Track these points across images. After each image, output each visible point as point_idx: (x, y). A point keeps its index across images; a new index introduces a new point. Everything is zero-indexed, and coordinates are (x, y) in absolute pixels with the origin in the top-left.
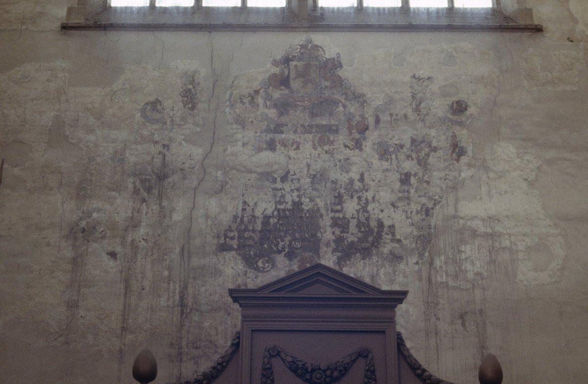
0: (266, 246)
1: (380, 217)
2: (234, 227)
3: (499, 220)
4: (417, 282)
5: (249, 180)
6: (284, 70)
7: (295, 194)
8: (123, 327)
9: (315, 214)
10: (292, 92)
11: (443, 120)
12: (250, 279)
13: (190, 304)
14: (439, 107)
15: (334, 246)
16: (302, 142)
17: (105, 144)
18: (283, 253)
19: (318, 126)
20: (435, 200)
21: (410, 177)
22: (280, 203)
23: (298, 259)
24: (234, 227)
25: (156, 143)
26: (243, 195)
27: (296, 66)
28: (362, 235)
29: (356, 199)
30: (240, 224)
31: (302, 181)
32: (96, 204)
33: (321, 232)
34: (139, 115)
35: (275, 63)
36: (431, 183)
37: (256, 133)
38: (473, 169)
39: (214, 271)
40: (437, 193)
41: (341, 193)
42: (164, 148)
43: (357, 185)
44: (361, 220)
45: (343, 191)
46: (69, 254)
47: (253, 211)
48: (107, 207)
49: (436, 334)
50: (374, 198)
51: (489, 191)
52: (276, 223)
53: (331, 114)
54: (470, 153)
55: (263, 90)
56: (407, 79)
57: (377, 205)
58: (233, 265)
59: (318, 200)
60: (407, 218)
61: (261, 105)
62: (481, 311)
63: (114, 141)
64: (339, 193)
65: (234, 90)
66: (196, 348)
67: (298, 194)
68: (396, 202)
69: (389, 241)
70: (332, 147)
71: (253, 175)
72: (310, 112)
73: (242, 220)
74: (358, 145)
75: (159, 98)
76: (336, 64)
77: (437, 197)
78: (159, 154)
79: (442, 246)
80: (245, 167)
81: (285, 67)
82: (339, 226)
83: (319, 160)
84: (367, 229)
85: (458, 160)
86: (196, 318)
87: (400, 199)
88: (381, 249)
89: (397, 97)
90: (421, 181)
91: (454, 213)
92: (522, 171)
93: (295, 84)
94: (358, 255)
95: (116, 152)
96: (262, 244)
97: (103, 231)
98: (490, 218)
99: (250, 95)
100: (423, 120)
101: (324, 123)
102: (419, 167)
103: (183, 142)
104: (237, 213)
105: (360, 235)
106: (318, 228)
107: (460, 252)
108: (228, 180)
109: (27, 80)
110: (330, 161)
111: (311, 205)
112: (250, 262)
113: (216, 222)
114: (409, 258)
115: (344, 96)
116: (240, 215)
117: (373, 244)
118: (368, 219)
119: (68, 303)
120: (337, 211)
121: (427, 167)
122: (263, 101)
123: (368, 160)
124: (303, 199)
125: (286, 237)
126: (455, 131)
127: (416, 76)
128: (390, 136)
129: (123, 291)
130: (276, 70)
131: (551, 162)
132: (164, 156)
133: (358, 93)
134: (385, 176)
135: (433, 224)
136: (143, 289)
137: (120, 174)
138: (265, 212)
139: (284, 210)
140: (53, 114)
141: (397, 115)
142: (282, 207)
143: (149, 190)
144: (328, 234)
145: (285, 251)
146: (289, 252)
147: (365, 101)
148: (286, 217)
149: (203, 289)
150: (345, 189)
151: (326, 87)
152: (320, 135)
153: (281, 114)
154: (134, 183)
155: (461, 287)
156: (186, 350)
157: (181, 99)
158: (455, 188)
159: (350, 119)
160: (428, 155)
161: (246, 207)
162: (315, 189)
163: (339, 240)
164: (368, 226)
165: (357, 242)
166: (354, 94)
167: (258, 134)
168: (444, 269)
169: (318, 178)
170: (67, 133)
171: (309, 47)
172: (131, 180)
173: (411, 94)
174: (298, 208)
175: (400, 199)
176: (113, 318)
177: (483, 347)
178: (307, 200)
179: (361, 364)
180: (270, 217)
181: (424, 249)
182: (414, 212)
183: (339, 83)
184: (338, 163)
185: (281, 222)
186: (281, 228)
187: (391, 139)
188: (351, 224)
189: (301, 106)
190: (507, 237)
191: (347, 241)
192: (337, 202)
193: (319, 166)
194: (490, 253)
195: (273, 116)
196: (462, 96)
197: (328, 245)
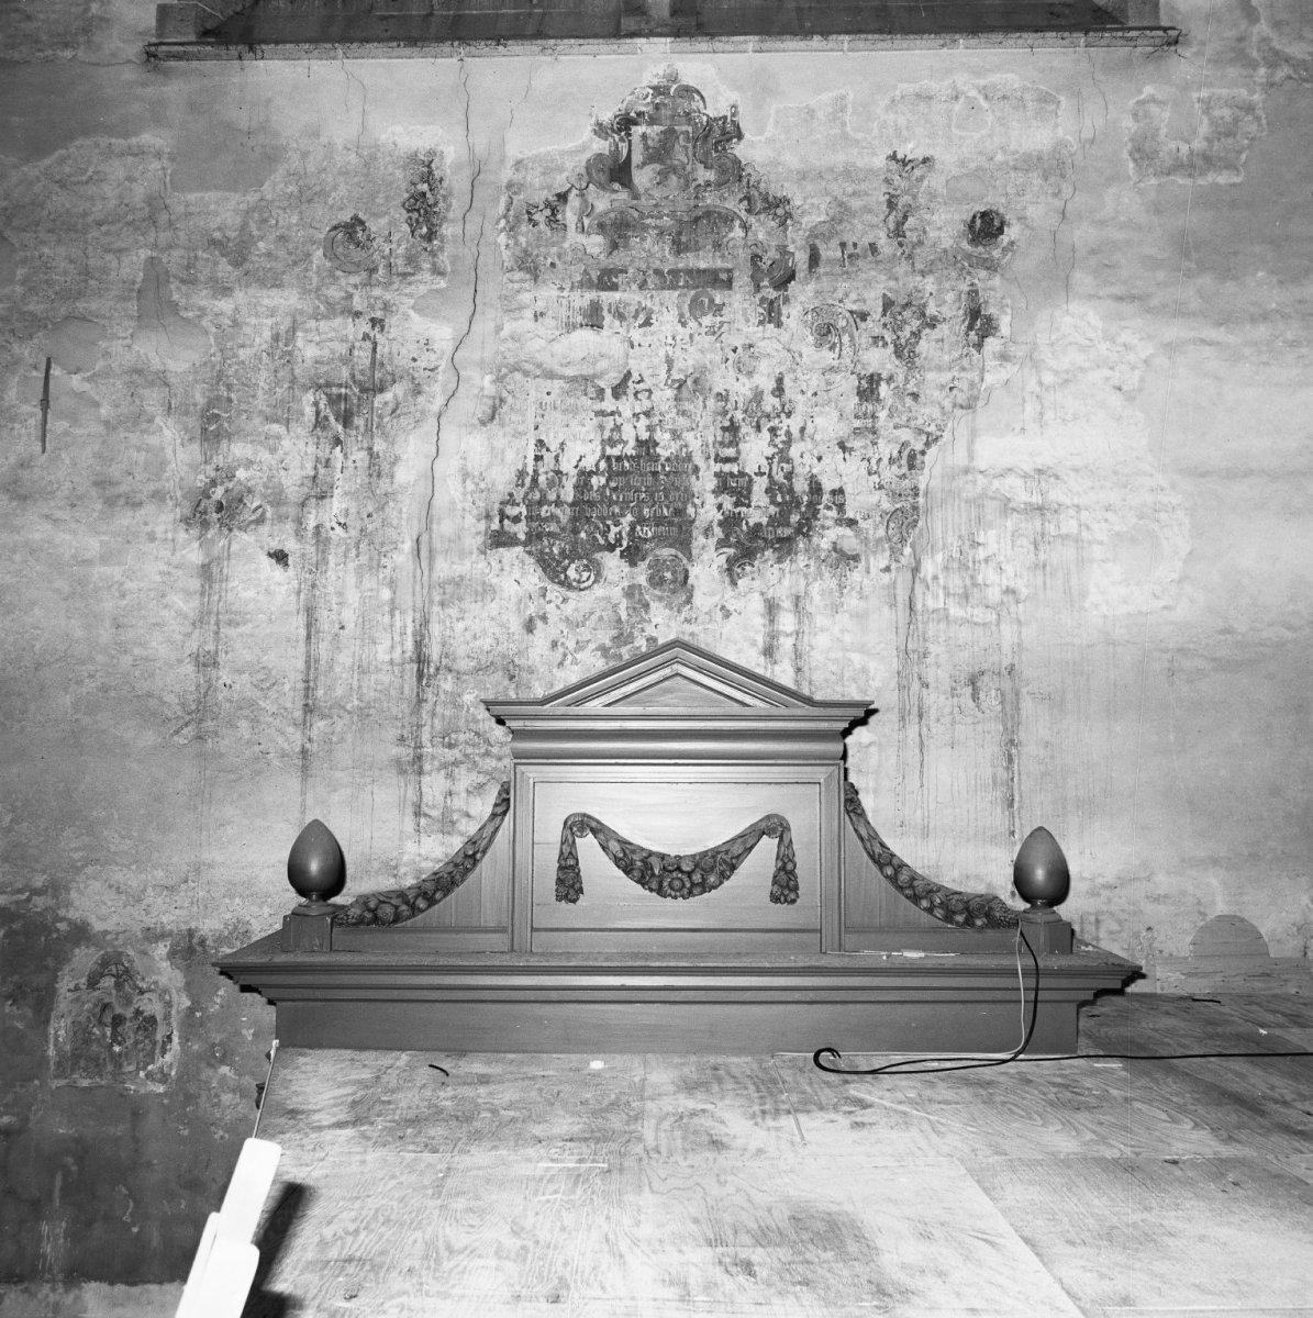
0: (583, 535)
1: (815, 471)
2: (519, 494)
3: (1057, 478)
4: (886, 609)
5: (548, 394)
6: (620, 145)
7: (644, 422)
8: (306, 705)
9: (683, 464)
10: (636, 197)
11: (950, 259)
12: (552, 605)
13: (435, 657)
14: (944, 226)
15: (722, 536)
16: (656, 308)
17: (253, 321)
18: (618, 550)
19: (689, 272)
20: (928, 434)
21: (878, 385)
22: (612, 442)
23: (647, 562)
24: (519, 496)
25: (358, 314)
26: (536, 428)
27: (644, 137)
28: (777, 510)
29: (766, 435)
30: (531, 489)
31: (656, 395)
32: (239, 450)
33: (695, 506)
34: (320, 252)
35: (601, 130)
36: (922, 399)
37: (562, 289)
38: (1009, 365)
39: (480, 589)
40: (933, 420)
41: (735, 420)
42: (373, 327)
43: (770, 403)
44: (776, 478)
45: (739, 416)
46: (195, 556)
47: (557, 461)
48: (264, 455)
49: (921, 716)
50: (803, 430)
51: (1041, 414)
52: (604, 487)
53: (717, 246)
54: (1005, 329)
55: (574, 192)
56: (880, 161)
57: (809, 445)
58: (517, 575)
59: (689, 437)
60: (870, 474)
61: (572, 227)
62: (1011, 670)
63: (272, 312)
64: (731, 420)
65: (515, 193)
66: (450, 746)
67: (648, 423)
68: (848, 440)
69: (829, 523)
70: (719, 319)
71: (557, 384)
72: (674, 242)
73: (535, 481)
74: (772, 314)
75: (361, 215)
76: (724, 133)
77: (932, 429)
78: (364, 339)
79: (939, 533)
80: (539, 366)
81: (622, 140)
82: (732, 492)
83: (691, 349)
84: (788, 497)
85: (979, 346)
86: (447, 684)
87: (857, 432)
88: (815, 540)
89: (856, 204)
90: (899, 393)
91: (966, 462)
92: (1112, 368)
93: (643, 177)
94: (768, 553)
95: (276, 338)
96: (576, 532)
97: (260, 507)
98: (1040, 471)
99: (548, 204)
100: (910, 257)
101: (703, 265)
102: (897, 362)
103: (411, 312)
104: (525, 465)
105: (773, 510)
106: (689, 495)
107: (975, 544)
108: (505, 394)
109: (84, 178)
110: (713, 351)
111: (674, 448)
112: (552, 568)
113: (482, 486)
114: (872, 559)
115: (746, 202)
116: (530, 470)
117: (799, 531)
118: (789, 476)
119: (198, 655)
120: (727, 460)
121: (914, 363)
122: (575, 219)
123: (793, 347)
124: (659, 436)
125: (623, 515)
126: (976, 281)
127: (899, 156)
128: (840, 295)
129: (303, 632)
130: (602, 146)
131: (1171, 348)
132: (375, 345)
133: (775, 198)
134: (828, 383)
135: (922, 487)
136: (342, 628)
137: (286, 386)
138: (581, 464)
139: (619, 459)
140: (144, 254)
141: (855, 245)
142: (615, 452)
143: (346, 420)
144: (708, 509)
145: (621, 545)
146: (628, 547)
147: (789, 215)
148: (624, 473)
149: (460, 626)
150: (746, 411)
151: (708, 184)
152: (693, 292)
153: (614, 246)
154: (316, 404)
155: (975, 619)
156: (430, 750)
157: (405, 215)
158: (969, 407)
159: (757, 256)
160: (916, 335)
161: (544, 451)
162: (684, 413)
163: (730, 522)
164: (791, 491)
165: (768, 525)
166: (766, 199)
167: (565, 294)
168: (941, 581)
169: (689, 387)
170: (176, 297)
171: (672, 90)
172: (309, 397)
173: (887, 197)
174: (648, 454)
175: (857, 432)
176: (287, 687)
177: (1012, 742)
178: (667, 436)
179: (767, 846)
180: (591, 473)
181: (903, 540)
182: (885, 461)
183: (733, 173)
184: (731, 355)
185: (613, 484)
186: (614, 497)
187: (841, 301)
188: (755, 488)
189: (656, 227)
190: (1072, 512)
191: (747, 523)
192: (727, 441)
193: (691, 362)
194: (1036, 548)
195: (595, 251)
196: (993, 200)
197: (707, 532)
